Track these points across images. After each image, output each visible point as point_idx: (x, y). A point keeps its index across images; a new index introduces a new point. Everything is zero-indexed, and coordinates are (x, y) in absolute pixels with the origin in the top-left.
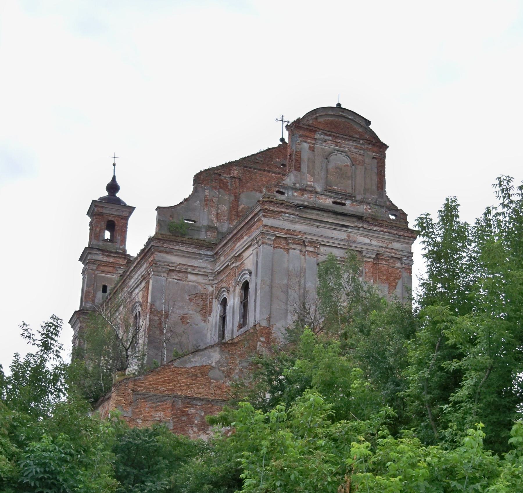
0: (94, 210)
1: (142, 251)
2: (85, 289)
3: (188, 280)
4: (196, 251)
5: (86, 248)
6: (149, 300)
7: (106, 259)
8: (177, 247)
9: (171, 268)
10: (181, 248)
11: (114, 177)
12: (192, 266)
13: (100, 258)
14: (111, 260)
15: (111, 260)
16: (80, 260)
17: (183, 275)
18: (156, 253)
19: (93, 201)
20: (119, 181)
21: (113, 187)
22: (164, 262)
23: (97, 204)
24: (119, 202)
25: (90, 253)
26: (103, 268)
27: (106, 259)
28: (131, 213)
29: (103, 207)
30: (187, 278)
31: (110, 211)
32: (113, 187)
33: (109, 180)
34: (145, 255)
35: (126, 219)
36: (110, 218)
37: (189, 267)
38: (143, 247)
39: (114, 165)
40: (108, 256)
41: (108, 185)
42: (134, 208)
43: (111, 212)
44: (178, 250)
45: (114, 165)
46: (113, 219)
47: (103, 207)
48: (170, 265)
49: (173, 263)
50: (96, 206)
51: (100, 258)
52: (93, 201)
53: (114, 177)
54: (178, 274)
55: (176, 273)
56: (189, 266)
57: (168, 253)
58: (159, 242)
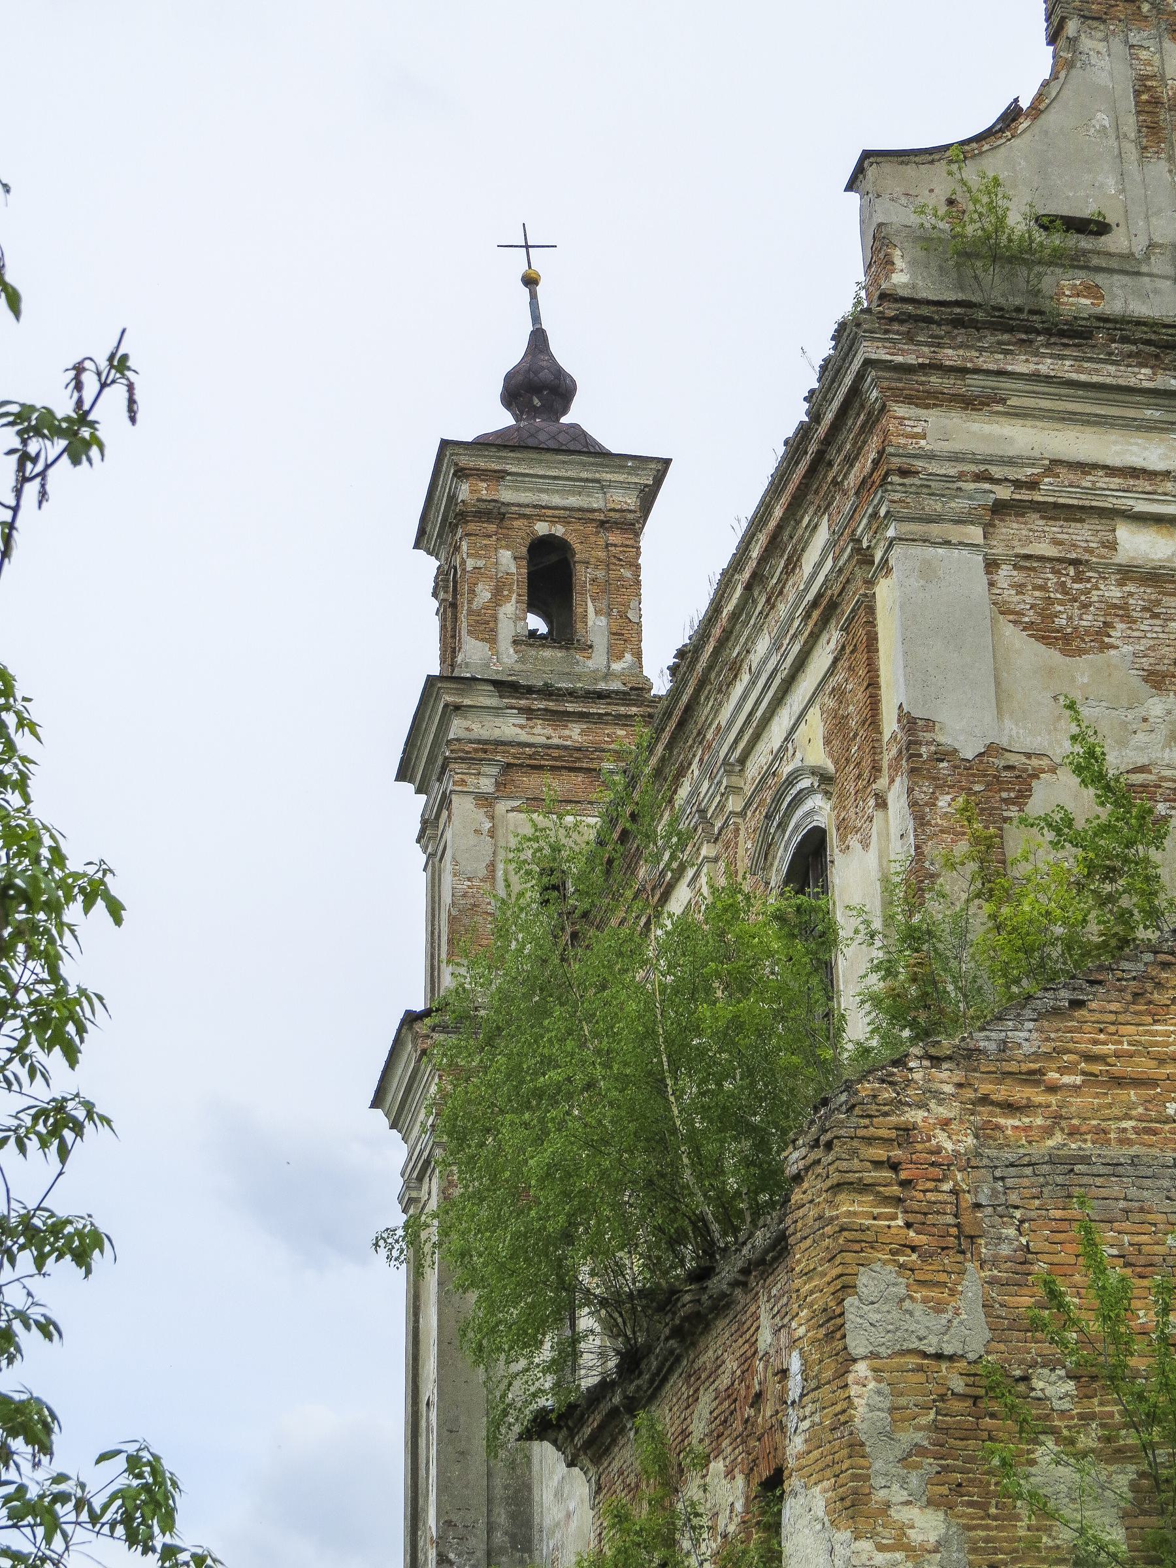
0: (452, 498)
1: (796, 446)
2: (447, 899)
3: (1121, 558)
4: (1142, 377)
5: (431, 681)
6: (892, 698)
7: (541, 733)
8: (1021, 365)
9: (1004, 493)
10: (1046, 367)
11: (539, 340)
12: (1135, 472)
13: (510, 728)
14: (575, 733)
15: (575, 733)
16: (403, 774)
17: (1083, 534)
18: (900, 410)
19: (445, 444)
20: (564, 353)
21: (539, 387)
22: (955, 458)
23: (465, 461)
24: (581, 447)
25: (458, 708)
26: (531, 782)
27: (541, 733)
28: (648, 497)
29: (500, 475)
30: (1112, 546)
31: (542, 495)
32: (539, 387)
33: (514, 353)
34: (820, 462)
35: (631, 525)
36: (542, 528)
37: (1115, 482)
38: (799, 413)
39: (530, 281)
40: (559, 718)
41: (509, 377)
42: (667, 462)
43: (545, 499)
44: (1035, 377)
45: (530, 281)
46: (559, 530)
47: (500, 475)
48: (997, 472)
49: (1010, 462)
50: (461, 473)
51: (510, 728)
52: (445, 444)
53: (539, 340)
54: (1054, 529)
55: (1036, 521)
56: (1112, 471)
57: (969, 403)
58: (910, 338)
